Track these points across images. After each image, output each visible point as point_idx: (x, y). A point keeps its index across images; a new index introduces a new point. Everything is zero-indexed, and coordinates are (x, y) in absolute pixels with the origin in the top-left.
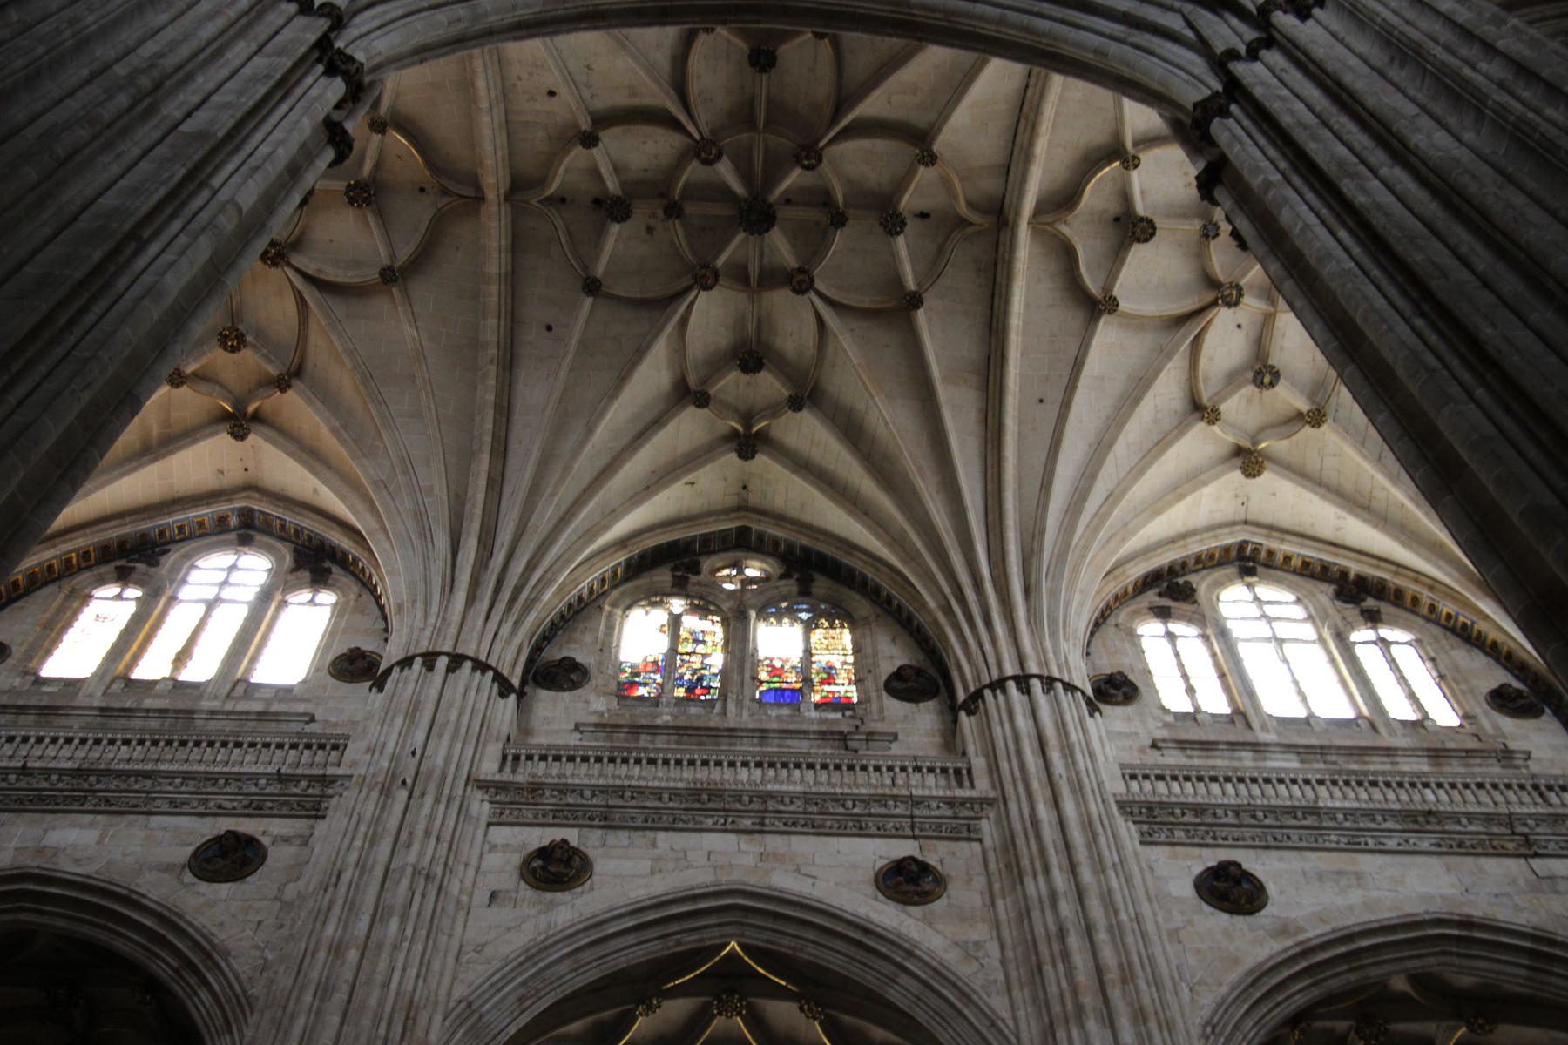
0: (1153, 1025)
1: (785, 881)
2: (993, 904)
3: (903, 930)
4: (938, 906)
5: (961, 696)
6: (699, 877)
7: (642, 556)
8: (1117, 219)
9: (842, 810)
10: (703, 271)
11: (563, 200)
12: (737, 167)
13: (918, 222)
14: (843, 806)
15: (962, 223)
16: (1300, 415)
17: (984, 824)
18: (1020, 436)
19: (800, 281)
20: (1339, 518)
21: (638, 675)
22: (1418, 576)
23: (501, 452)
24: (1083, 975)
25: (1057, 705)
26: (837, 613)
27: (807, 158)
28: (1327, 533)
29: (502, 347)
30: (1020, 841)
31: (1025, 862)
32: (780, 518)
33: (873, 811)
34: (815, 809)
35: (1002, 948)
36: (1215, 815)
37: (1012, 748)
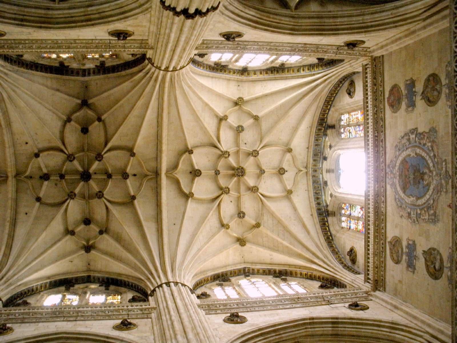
3: (121, 336)
7: (55, 282)
8: (191, 172)
9: (104, 314)
10: (71, 194)
11: (31, 177)
12: (80, 164)
13: (134, 177)
14: (105, 313)
15: (146, 176)
19: (100, 195)
20: (271, 255)
22: (295, 266)
23: (9, 247)
25: (179, 291)
27: (99, 157)
28: (268, 261)
29: (12, 219)
32: (100, 272)
33: (115, 313)
34: (95, 314)
36: (230, 306)
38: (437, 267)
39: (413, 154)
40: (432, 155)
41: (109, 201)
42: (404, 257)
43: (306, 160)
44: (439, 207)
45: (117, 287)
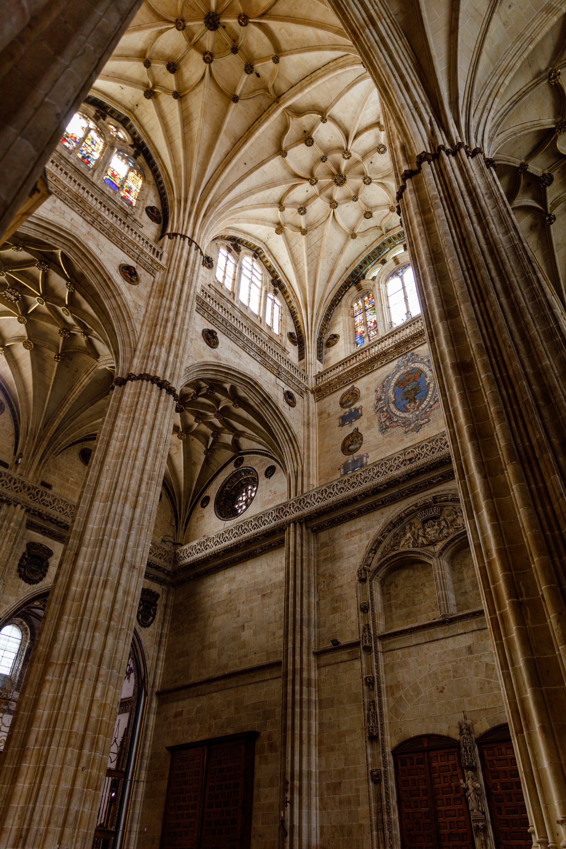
0: (178, 360)
1: (92, 245)
2: (149, 297)
3: (121, 287)
4: (134, 287)
5: (169, 231)
6: (65, 224)
8: (305, 132)
10: (181, 22)
15: (266, 89)
16: (301, 228)
17: (158, 273)
18: (232, 169)
19: (208, 58)
21: (68, 137)
22: (293, 291)
24: (168, 335)
26: (141, 172)
27: (243, 20)
28: (281, 263)
30: (168, 286)
31: (166, 293)
32: (142, 126)
34: (112, 231)
35: (146, 312)
37: (178, 258)
38: (352, 447)
39: (427, 379)
40: (431, 403)
41: (210, 72)
42: (347, 410)
43: (394, 226)
44: (394, 430)
45: (145, 164)
